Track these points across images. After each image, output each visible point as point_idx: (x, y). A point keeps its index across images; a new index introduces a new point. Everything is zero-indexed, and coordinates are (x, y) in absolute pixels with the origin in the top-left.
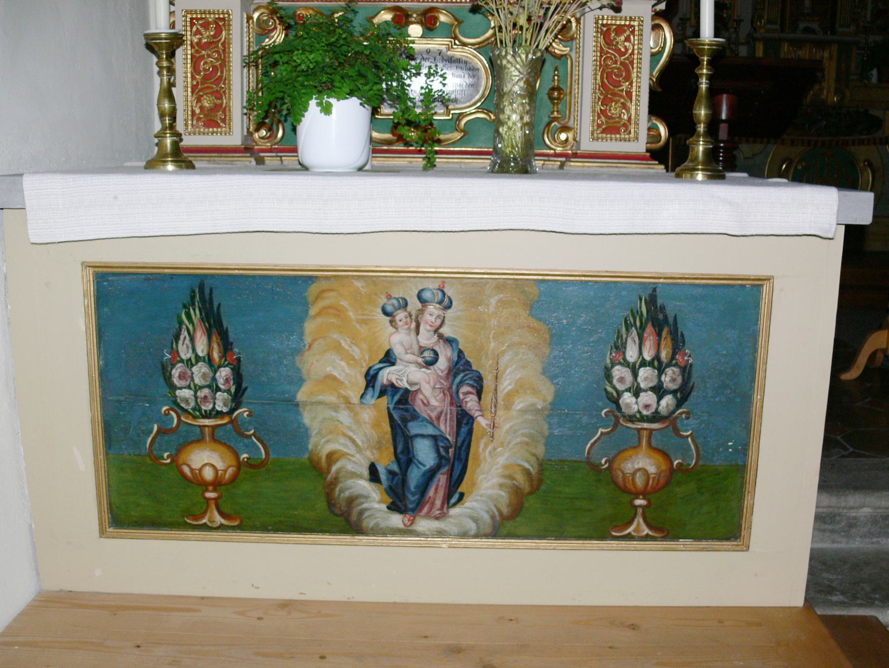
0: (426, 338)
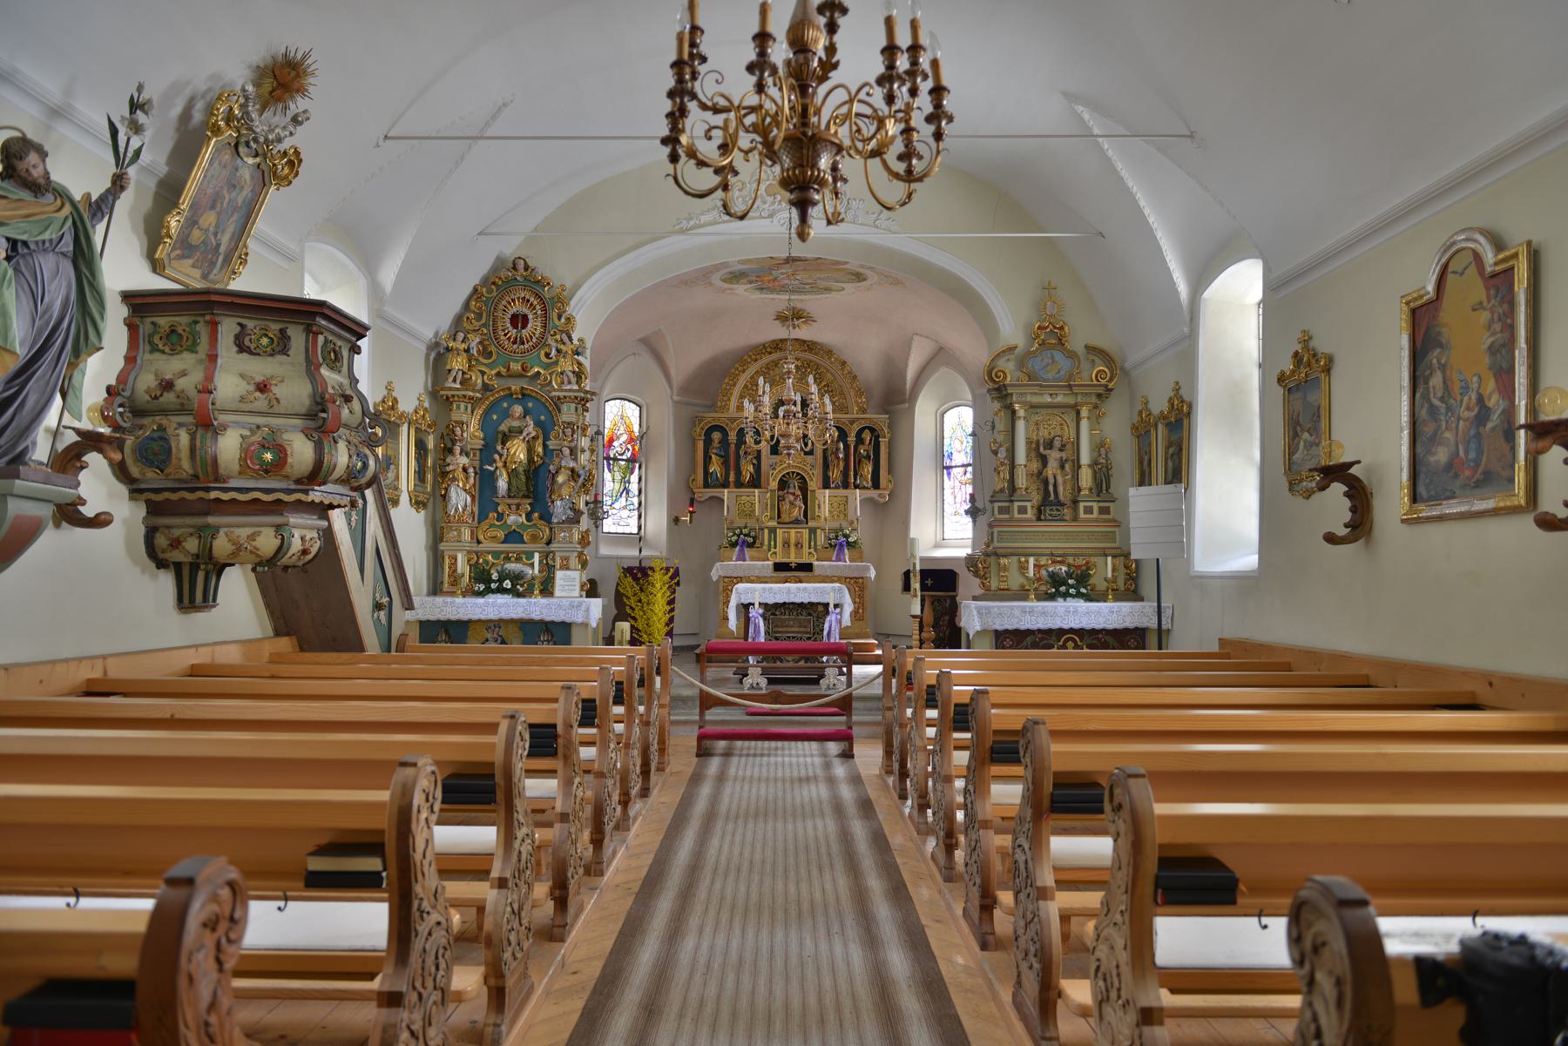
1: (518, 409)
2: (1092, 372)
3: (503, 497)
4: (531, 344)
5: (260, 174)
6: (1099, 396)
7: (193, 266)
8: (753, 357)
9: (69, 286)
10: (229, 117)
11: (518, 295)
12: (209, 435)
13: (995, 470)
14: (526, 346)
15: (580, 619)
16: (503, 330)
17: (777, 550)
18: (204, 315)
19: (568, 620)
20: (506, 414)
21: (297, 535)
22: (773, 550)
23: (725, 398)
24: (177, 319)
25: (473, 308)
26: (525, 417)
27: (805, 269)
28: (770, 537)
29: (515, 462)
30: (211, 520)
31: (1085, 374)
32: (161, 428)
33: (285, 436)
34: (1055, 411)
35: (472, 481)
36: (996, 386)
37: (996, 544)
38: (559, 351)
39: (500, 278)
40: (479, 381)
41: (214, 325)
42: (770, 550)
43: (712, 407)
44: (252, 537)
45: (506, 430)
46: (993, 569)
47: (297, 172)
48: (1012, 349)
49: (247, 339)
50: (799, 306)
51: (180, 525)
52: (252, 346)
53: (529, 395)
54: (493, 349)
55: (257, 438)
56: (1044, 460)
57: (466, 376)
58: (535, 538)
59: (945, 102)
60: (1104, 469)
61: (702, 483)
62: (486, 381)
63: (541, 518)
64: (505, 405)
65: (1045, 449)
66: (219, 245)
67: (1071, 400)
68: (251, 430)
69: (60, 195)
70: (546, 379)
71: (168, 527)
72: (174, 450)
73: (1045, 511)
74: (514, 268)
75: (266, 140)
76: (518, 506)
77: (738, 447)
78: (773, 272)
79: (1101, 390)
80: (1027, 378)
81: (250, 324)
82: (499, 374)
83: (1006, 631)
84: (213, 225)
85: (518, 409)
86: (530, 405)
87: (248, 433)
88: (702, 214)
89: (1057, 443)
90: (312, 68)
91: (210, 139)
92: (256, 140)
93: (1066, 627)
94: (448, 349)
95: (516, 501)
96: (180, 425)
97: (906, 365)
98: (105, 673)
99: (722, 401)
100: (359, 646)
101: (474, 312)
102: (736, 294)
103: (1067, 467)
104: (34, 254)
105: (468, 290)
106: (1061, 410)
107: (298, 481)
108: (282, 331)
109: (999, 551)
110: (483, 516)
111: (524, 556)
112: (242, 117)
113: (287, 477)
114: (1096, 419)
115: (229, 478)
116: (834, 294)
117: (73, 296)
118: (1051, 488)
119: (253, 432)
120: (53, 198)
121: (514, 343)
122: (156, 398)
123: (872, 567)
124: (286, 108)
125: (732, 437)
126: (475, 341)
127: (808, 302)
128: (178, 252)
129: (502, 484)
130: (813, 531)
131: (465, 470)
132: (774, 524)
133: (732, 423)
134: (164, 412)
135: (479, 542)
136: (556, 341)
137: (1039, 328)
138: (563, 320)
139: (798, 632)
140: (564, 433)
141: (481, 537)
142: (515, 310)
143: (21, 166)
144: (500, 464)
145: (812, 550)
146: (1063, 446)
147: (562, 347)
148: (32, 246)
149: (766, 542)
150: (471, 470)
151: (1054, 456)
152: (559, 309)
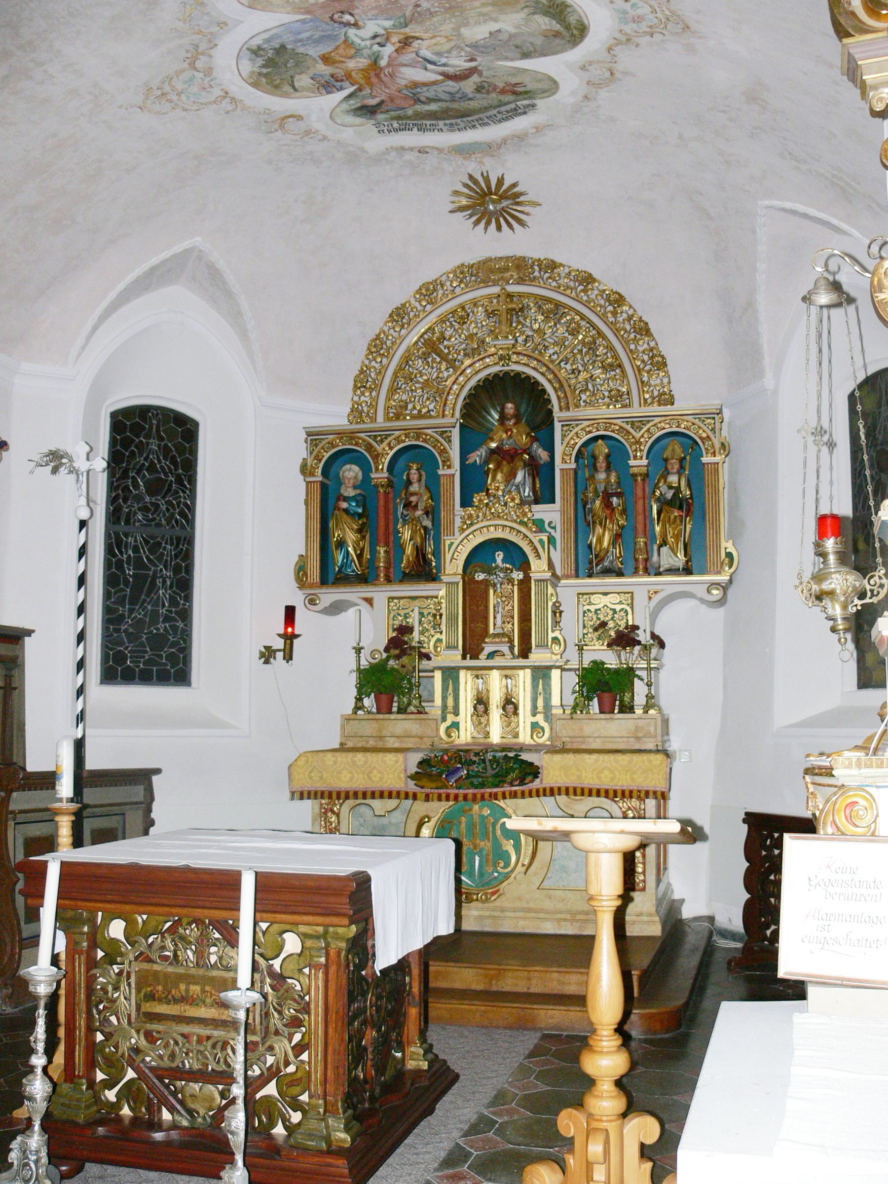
22: (450, 718)
28: (445, 689)
42: (444, 719)
130: (541, 673)
145: (540, 719)
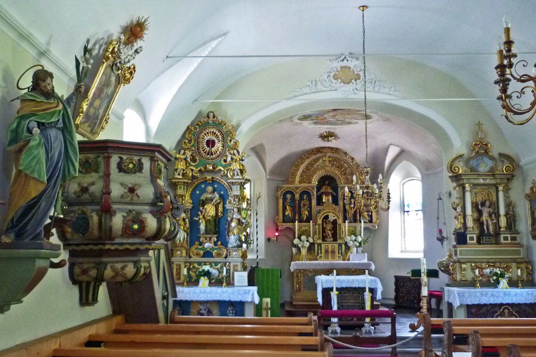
0: (205, 307)
1: (210, 188)
2: (503, 168)
3: (203, 234)
4: (216, 155)
5: (119, 78)
6: (508, 179)
7: (88, 126)
8: (307, 156)
9: (61, 145)
10: (113, 52)
11: (210, 130)
12: (108, 216)
13: (455, 218)
14: (214, 156)
15: (249, 299)
16: (203, 148)
17: (322, 255)
18: (104, 153)
19: (243, 300)
20: (204, 191)
21: (143, 264)
22: (320, 255)
23: (293, 177)
24: (89, 155)
25: (187, 137)
26: (214, 192)
27: (341, 114)
28: (318, 248)
29: (209, 216)
30: (104, 260)
31: (500, 168)
32: (83, 213)
33: (144, 216)
34: (485, 187)
35: (188, 225)
36: (455, 175)
37: (459, 257)
38: (232, 159)
39: (201, 122)
40: (190, 174)
41: (108, 159)
42: (318, 255)
43: (286, 181)
44: (123, 268)
45: (204, 199)
46: (458, 270)
47: (133, 76)
48: (461, 156)
49: (123, 165)
50: (332, 131)
51: (87, 263)
52: (126, 168)
53: (216, 181)
54: (197, 158)
55: (130, 217)
56: (480, 213)
57: (184, 172)
58: (219, 255)
59: (512, 48)
60: (512, 217)
61: (282, 220)
62: (194, 174)
63: (222, 244)
64: (203, 186)
65: (482, 206)
66: (99, 115)
67: (493, 182)
68: (127, 213)
69: (56, 98)
70: (224, 173)
71: (81, 263)
72: (91, 225)
73: (483, 239)
74: (208, 117)
75: (125, 62)
76: (210, 238)
77: (300, 201)
78: (325, 115)
79: (509, 177)
80: (469, 170)
81: (125, 157)
82: (200, 171)
83: (474, 305)
84: (98, 105)
85: (210, 188)
86: (216, 186)
87: (125, 214)
88: (297, 89)
89: (487, 204)
90: (147, 26)
91: (104, 63)
92: (120, 62)
93: (504, 302)
94: (176, 158)
95: (209, 236)
96: (93, 211)
97: (385, 159)
98: (60, 345)
99: (291, 178)
100: (157, 321)
101: (188, 139)
102: (303, 126)
103: (493, 216)
104: (47, 129)
105: (184, 129)
106: (488, 186)
107: (148, 239)
108: (139, 160)
109: (462, 261)
110: (192, 244)
111: (213, 264)
112: (117, 52)
113: (143, 237)
114: (507, 190)
115: (115, 238)
116: (352, 126)
117: (63, 151)
118: (485, 227)
119: (128, 215)
120: (53, 100)
121: (208, 154)
122: (79, 196)
123: (373, 264)
124: (133, 46)
125: (297, 196)
126: (189, 154)
127: (338, 129)
128: (84, 120)
129: (202, 227)
131: (184, 220)
132: (320, 241)
133: (297, 190)
134: (83, 204)
135: (190, 257)
136: (231, 154)
137: (475, 145)
138: (232, 142)
139: (353, 303)
140: (234, 200)
141: (191, 255)
142: (209, 138)
143: (43, 84)
144: (201, 217)
145: (340, 255)
146: (491, 205)
147: (234, 157)
148: (46, 126)
149: (316, 251)
150: (187, 220)
151: (486, 211)
152: (231, 137)
